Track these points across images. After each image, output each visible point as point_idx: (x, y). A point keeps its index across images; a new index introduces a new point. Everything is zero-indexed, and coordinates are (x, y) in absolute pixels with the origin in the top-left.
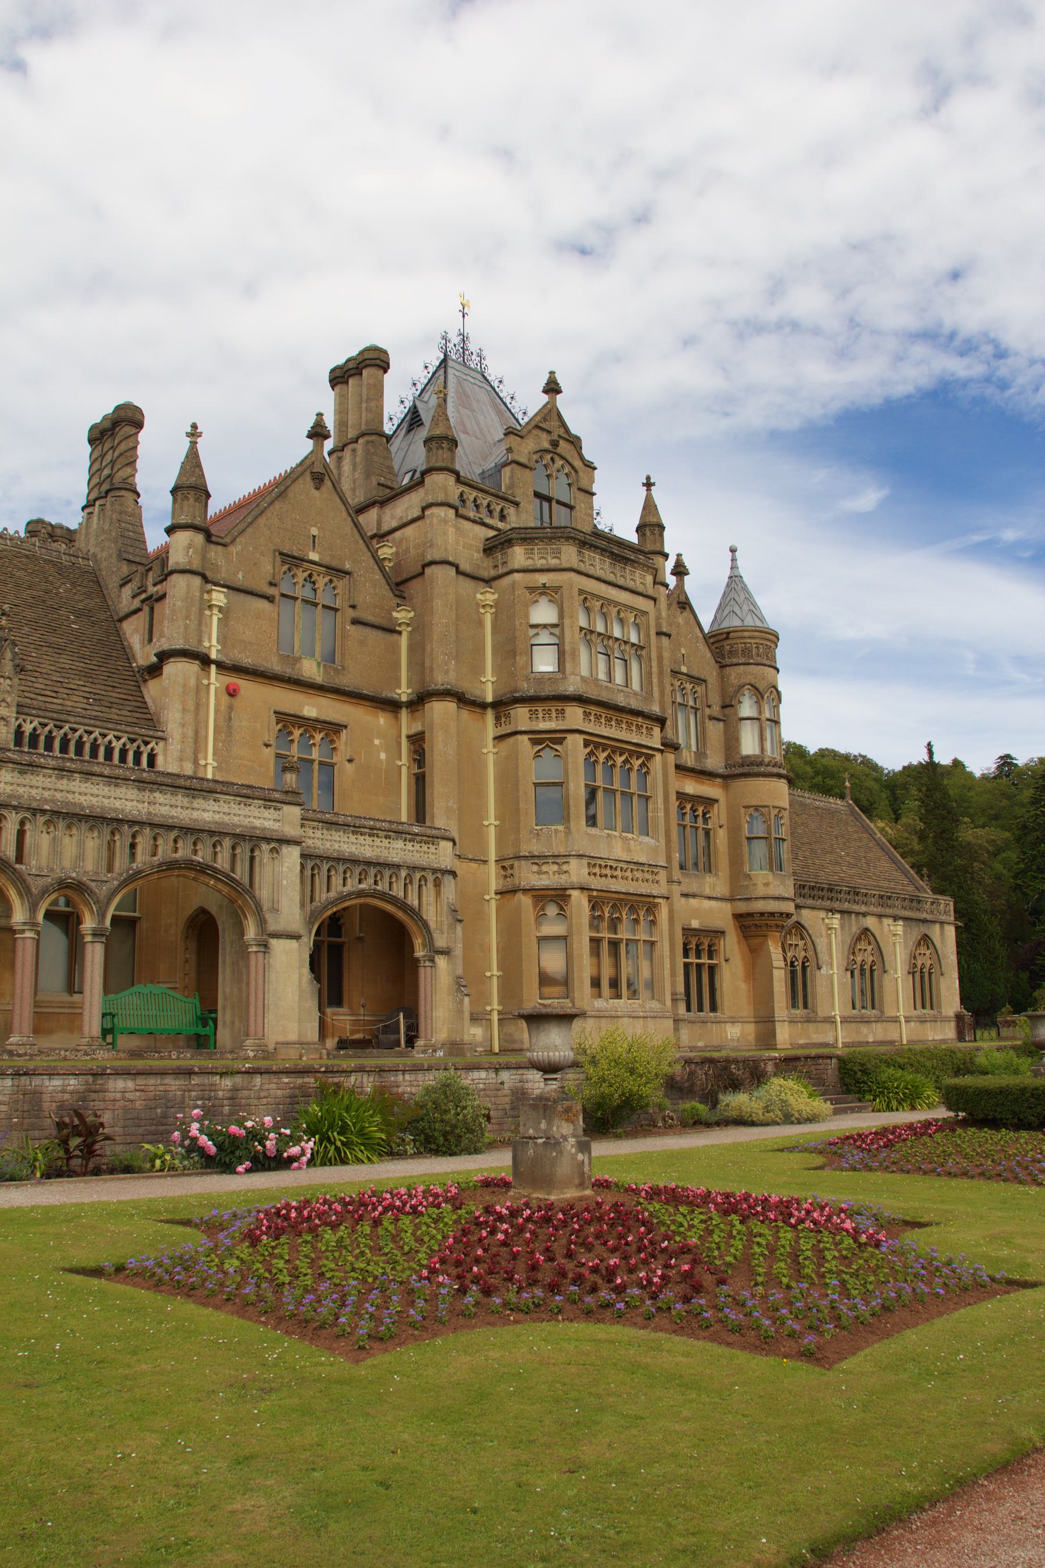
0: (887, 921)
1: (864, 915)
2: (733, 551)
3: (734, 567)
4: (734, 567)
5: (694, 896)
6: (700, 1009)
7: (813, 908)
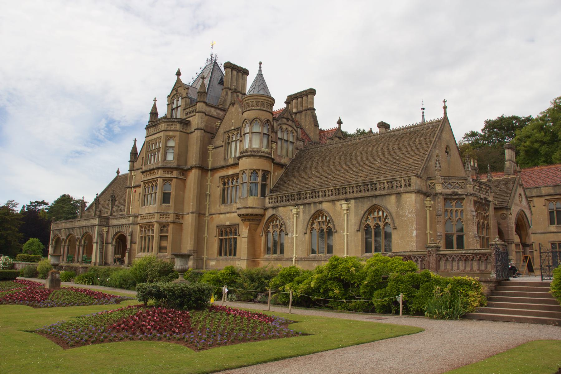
0: (338, 203)
1: (320, 203)
2: (260, 63)
3: (260, 70)
4: (260, 70)
5: (228, 213)
6: (230, 255)
7: (285, 206)
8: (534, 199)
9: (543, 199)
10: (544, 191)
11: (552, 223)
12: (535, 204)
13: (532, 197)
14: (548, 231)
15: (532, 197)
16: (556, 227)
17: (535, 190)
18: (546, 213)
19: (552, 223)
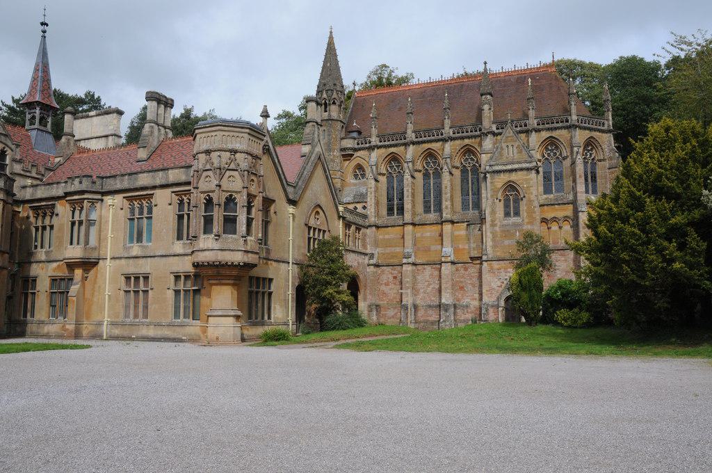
8: (158, 192)
9: (169, 191)
10: (174, 175)
11: (179, 237)
12: (158, 203)
13: (154, 187)
14: (172, 252)
15: (154, 187)
16: (184, 244)
17: (160, 173)
18: (171, 219)
19: (179, 237)
